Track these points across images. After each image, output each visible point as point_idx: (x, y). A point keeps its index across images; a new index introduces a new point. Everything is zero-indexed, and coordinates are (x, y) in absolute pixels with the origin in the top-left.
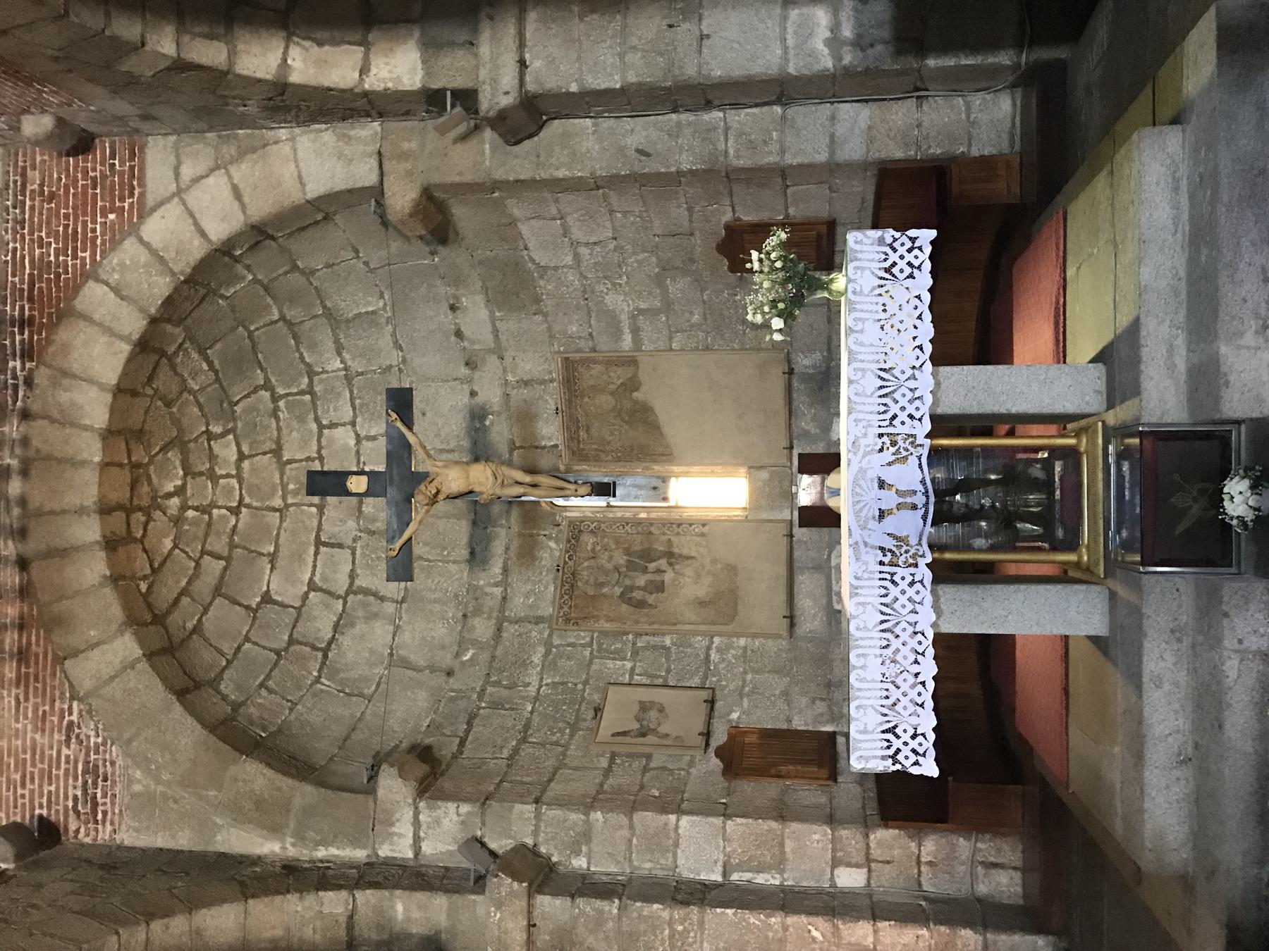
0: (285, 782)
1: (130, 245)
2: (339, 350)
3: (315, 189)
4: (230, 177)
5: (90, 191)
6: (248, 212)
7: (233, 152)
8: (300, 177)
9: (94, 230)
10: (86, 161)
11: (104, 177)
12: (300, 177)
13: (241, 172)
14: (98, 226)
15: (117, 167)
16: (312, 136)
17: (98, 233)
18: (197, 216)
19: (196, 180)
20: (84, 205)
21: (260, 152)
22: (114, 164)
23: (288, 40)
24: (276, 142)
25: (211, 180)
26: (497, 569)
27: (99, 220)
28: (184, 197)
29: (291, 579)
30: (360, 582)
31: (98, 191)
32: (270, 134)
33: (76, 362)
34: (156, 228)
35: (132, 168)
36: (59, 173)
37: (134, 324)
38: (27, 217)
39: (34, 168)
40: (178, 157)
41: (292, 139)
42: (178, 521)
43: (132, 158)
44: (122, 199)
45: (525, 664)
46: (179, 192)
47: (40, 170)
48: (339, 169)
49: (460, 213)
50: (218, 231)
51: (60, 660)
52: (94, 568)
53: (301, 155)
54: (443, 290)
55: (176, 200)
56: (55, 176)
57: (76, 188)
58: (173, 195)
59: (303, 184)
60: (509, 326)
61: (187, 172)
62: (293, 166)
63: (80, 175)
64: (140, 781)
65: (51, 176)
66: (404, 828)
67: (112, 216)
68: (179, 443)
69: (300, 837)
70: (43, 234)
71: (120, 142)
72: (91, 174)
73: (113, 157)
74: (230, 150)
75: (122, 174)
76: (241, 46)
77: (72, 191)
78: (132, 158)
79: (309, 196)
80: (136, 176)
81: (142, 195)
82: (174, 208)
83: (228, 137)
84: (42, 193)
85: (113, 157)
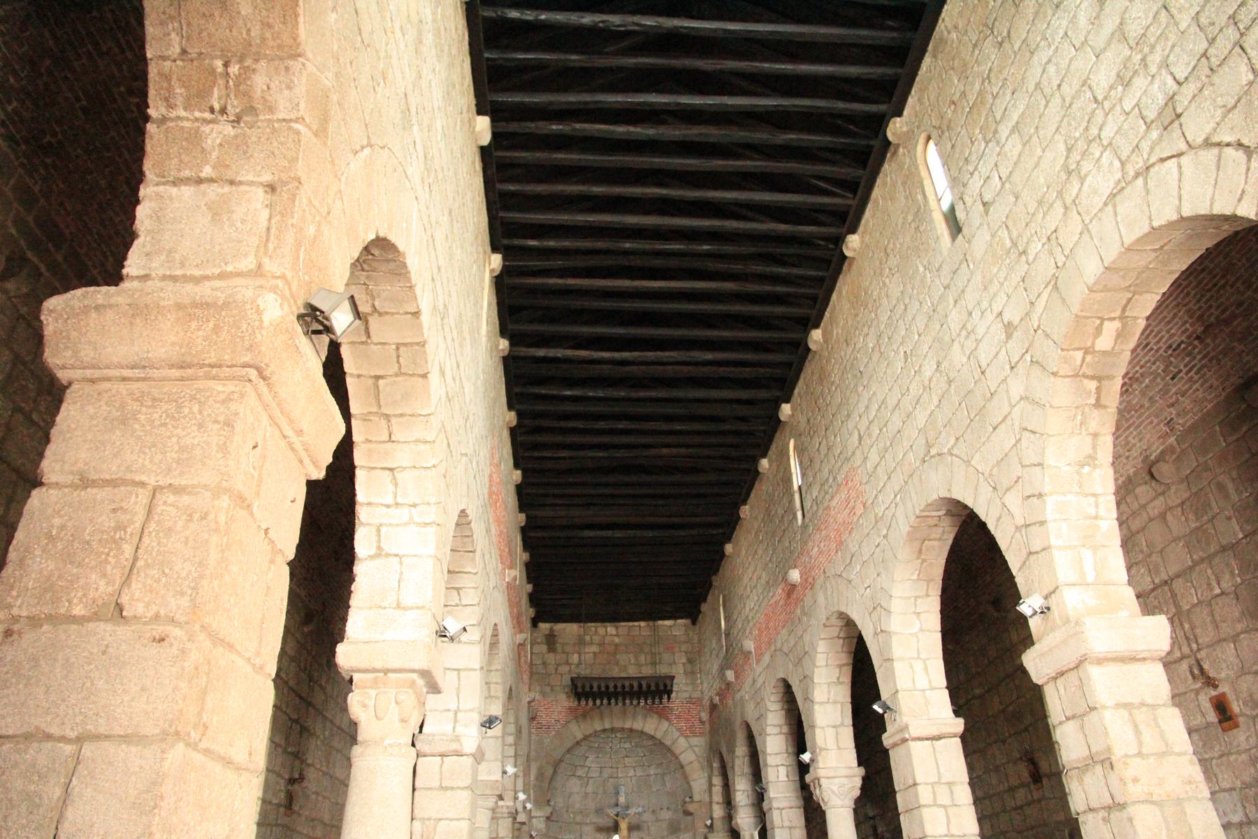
0: (547, 781)
1: (678, 734)
2: (656, 774)
3: (692, 783)
20: (687, 720)
26: (594, 820)
29: (592, 762)
30: (591, 781)
33: (649, 719)
34: (682, 740)
37: (659, 735)
42: (608, 737)
45: (570, 833)
46: (691, 747)
49: (689, 818)
50: (682, 758)
51: (576, 718)
52: (598, 727)
54: (673, 806)
60: (664, 825)
61: (696, 749)
64: (547, 741)
66: (539, 813)
68: (629, 737)
69: (535, 786)
74: (701, 760)
80: (694, 734)
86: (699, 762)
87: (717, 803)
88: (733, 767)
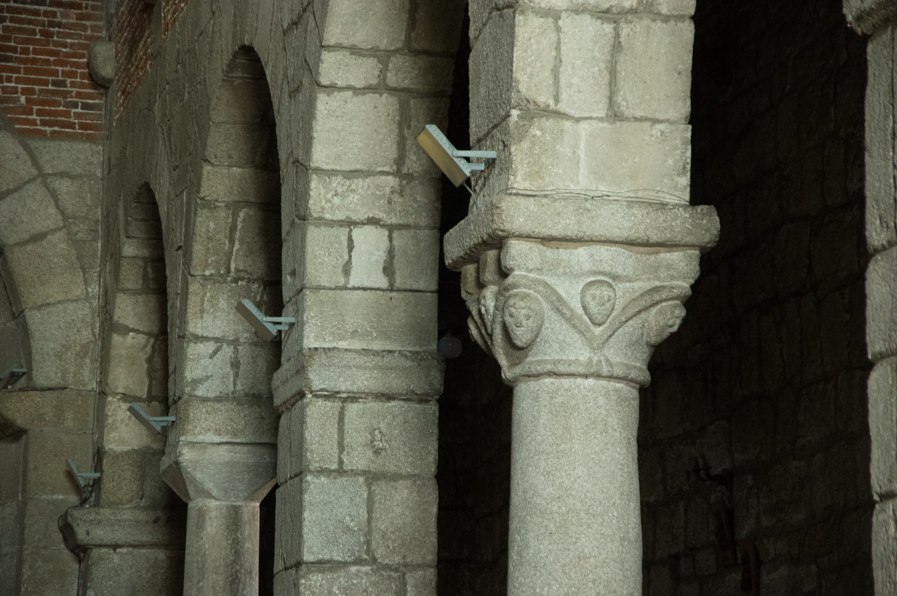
3: (34, 319)
4: (53, 231)
5: (51, 78)
6: (16, 250)
7: (80, 236)
8: (48, 305)
9: (9, 80)
10: (83, 76)
11: (65, 94)
12: (48, 305)
13: (58, 243)
14: (13, 84)
15: (74, 110)
16: (88, 319)
17: (6, 84)
18: (16, 195)
19: (53, 194)
21: (77, 265)
22: (76, 107)
23: (149, 334)
24: (86, 281)
25: (52, 210)
27: (20, 86)
28: (39, 180)
31: (50, 87)
32: (94, 273)
35: (71, 125)
36: (72, 46)
38: (28, 6)
39: (80, 17)
40: (80, 176)
41: (87, 298)
43: (83, 126)
44: (40, 113)
47: (77, 24)
48: (52, 345)
53: (71, 306)
55: (35, 172)
56: (69, 41)
57: (56, 63)
58: (39, 169)
59: (39, 308)
61: (64, 186)
62: (60, 297)
63: (68, 69)
65: (70, 36)
67: (23, 99)
70: (7, 23)
71: (100, 115)
72: (69, 80)
73: (85, 106)
74: (81, 231)
75: (67, 114)
76: (141, 298)
77: (52, 59)
78: (83, 126)
79: (27, 313)
81: (43, 134)
82: (26, 169)
83: (96, 231)
84: (52, 24)
85: (85, 106)
86: (75, 243)
87: (125, 397)
88: (186, 249)
